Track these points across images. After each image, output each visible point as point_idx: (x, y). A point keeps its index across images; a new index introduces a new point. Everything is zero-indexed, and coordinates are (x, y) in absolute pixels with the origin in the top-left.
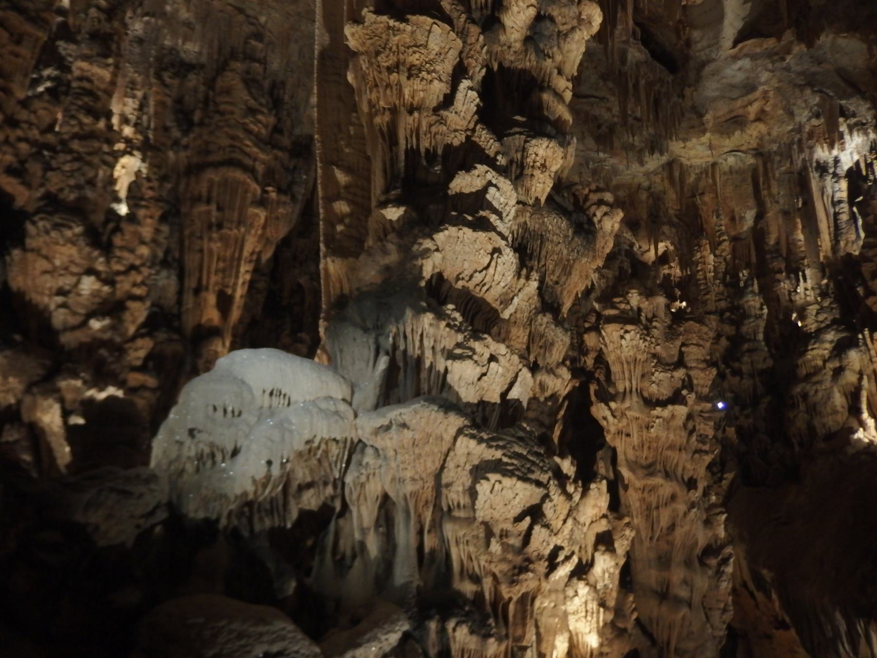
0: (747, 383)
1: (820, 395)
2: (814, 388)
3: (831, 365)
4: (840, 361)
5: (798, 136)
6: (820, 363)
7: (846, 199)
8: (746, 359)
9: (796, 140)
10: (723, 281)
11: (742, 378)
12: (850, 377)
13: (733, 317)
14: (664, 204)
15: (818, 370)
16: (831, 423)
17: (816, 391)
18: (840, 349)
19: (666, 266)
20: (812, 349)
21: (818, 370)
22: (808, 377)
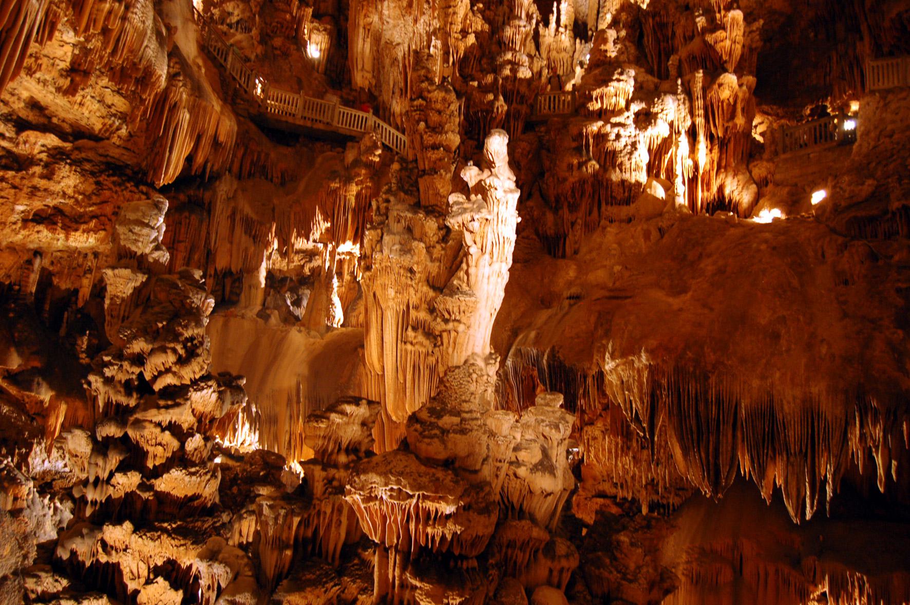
1: (623, 141)
2: (616, 130)
4: (651, 103)
6: (622, 104)
17: (618, 136)
20: (619, 80)
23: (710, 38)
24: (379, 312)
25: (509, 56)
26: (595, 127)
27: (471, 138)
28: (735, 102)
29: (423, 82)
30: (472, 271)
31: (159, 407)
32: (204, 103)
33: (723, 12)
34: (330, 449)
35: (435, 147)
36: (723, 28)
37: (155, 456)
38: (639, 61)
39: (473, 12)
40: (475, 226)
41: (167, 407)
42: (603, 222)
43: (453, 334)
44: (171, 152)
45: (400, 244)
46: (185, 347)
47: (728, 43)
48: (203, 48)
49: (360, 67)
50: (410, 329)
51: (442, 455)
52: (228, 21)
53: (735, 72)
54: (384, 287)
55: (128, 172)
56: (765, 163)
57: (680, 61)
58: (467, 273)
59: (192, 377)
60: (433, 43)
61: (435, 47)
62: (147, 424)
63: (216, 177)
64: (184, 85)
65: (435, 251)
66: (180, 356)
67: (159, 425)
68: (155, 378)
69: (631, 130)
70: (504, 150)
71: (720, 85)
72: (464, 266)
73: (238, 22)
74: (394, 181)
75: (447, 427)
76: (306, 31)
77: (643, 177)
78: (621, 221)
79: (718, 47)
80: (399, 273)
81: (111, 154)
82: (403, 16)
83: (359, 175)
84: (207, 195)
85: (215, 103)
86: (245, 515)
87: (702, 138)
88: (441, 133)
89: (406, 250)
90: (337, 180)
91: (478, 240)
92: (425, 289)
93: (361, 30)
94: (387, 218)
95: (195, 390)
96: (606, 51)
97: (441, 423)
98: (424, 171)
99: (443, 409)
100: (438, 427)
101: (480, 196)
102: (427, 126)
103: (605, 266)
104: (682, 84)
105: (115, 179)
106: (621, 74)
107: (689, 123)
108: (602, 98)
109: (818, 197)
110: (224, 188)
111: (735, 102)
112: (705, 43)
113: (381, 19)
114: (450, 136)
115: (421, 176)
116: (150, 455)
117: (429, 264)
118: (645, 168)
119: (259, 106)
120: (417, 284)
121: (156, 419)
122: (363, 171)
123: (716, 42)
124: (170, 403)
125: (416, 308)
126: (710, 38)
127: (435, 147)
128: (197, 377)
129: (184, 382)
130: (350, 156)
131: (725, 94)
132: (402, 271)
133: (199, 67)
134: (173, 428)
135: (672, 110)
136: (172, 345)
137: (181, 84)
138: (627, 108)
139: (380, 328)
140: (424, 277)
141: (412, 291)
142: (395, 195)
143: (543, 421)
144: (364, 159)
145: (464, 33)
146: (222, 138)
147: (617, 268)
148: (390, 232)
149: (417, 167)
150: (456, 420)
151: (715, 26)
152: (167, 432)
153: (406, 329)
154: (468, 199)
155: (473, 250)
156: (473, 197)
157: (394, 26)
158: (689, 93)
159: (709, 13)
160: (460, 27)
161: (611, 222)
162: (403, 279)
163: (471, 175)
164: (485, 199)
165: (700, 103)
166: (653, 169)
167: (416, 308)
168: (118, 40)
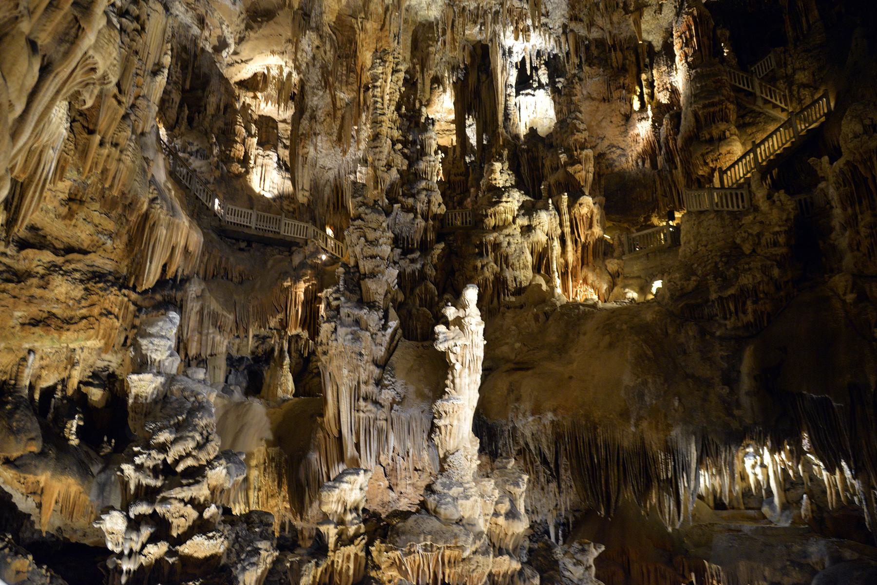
0: (420, 222)
1: (513, 246)
2: (507, 239)
3: (523, 221)
5: (498, 7)
6: (510, 218)
7: (514, 85)
8: (423, 196)
9: (494, 10)
10: (398, 109)
11: (416, 217)
12: (540, 236)
13: (406, 151)
14: (321, 6)
15: (505, 225)
16: (523, 278)
18: (528, 210)
19: (252, 94)
20: (507, 202)
21: (505, 225)
22: (496, 228)
23: (570, 170)
24: (335, 388)
25: (423, 184)
26: (491, 237)
27: (397, 247)
28: (592, 216)
29: (360, 206)
30: (457, 381)
31: (182, 486)
32: (177, 221)
33: (579, 151)
34: (339, 511)
35: (373, 257)
36: (580, 163)
37: (179, 526)
38: (519, 185)
39: (394, 150)
40: (457, 350)
41: (189, 485)
42: (502, 309)
43: (449, 427)
44: (151, 263)
45: (352, 334)
46: (202, 434)
47: (584, 173)
48: (172, 174)
49: (300, 188)
50: (361, 400)
51: (456, 517)
52: (189, 150)
53: (590, 194)
54: (340, 368)
55: (110, 278)
56: (616, 261)
57: (549, 185)
58: (453, 382)
59: (207, 458)
60: (359, 169)
61: (360, 172)
62: (172, 501)
63: (186, 280)
64: (162, 207)
65: (378, 337)
66: (198, 443)
67: (182, 500)
68: (177, 462)
69: (519, 238)
70: (476, 298)
71: (581, 205)
72: (450, 377)
73: (197, 151)
74: (341, 283)
75: (455, 495)
76: (252, 157)
77: (529, 273)
78: (516, 307)
79: (577, 176)
80: (351, 357)
81: (96, 264)
82: (334, 147)
83: (306, 275)
84: (179, 295)
85: (185, 220)
86: (248, 567)
87: (569, 243)
88: (377, 246)
89: (356, 339)
90: (289, 280)
91: (460, 359)
92: (372, 367)
93: (300, 158)
94: (339, 313)
95: (210, 469)
96: (495, 179)
97: (451, 493)
98: (365, 274)
99: (451, 483)
100: (450, 496)
101: (457, 327)
102: (367, 241)
103: (507, 343)
104: (553, 203)
105: (101, 285)
106: (508, 197)
107: (559, 231)
108: (495, 215)
109: (657, 284)
110: (194, 289)
111: (592, 216)
112: (567, 172)
113: (316, 149)
114: (384, 247)
115: (363, 279)
116: (174, 525)
117: (374, 348)
118: (530, 267)
119: (220, 220)
120: (365, 364)
121: (180, 496)
122: (309, 272)
123: (575, 173)
124: (191, 481)
125: (366, 383)
126: (570, 170)
127: (373, 257)
128: (212, 457)
129: (201, 463)
130: (297, 259)
131: (584, 210)
132: (353, 355)
133: (169, 190)
134: (192, 502)
135: (546, 220)
136: (191, 434)
137: (158, 206)
138: (514, 221)
139: (336, 400)
140: (370, 359)
141: (362, 370)
142: (343, 295)
143: (508, 481)
144: (309, 262)
145: (389, 166)
146: (191, 249)
147: (517, 345)
148: (343, 325)
149: (359, 271)
150: (461, 489)
151: (574, 161)
152: (189, 506)
153: (358, 400)
154: (448, 328)
155: (458, 366)
156: (452, 327)
157: (327, 155)
158: (558, 209)
159: (568, 151)
160: (384, 162)
161: (508, 308)
162: (355, 361)
163: (451, 312)
164: (462, 328)
165: (566, 217)
166: (537, 269)
167: (366, 383)
168: (114, 178)
